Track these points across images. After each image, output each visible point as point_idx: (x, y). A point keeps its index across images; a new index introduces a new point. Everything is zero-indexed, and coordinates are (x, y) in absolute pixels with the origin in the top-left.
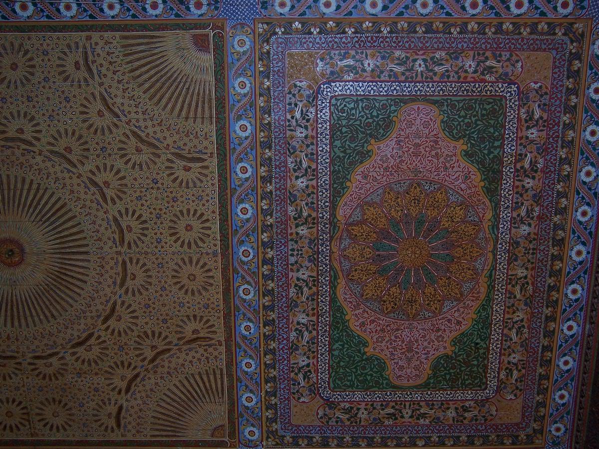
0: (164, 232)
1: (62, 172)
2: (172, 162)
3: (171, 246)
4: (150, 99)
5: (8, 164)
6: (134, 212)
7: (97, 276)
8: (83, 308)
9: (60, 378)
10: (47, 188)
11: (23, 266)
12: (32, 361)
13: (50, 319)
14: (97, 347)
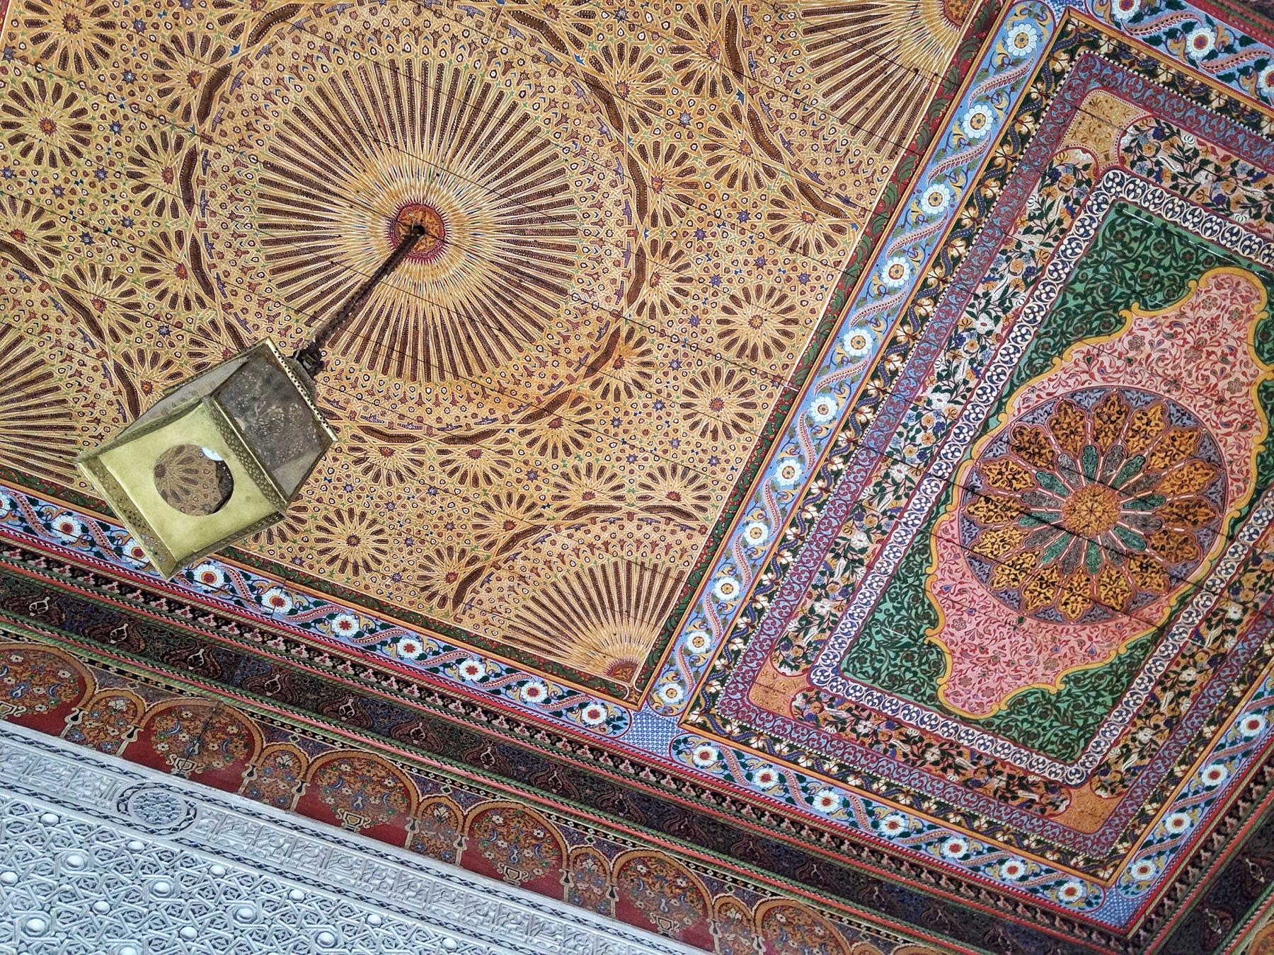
0: (101, 140)
1: (257, 327)
2: (44, 259)
3: (95, 106)
4: (50, 375)
6: (146, 203)
8: (325, 61)
10: (298, 311)
11: (407, 197)
13: (402, 68)
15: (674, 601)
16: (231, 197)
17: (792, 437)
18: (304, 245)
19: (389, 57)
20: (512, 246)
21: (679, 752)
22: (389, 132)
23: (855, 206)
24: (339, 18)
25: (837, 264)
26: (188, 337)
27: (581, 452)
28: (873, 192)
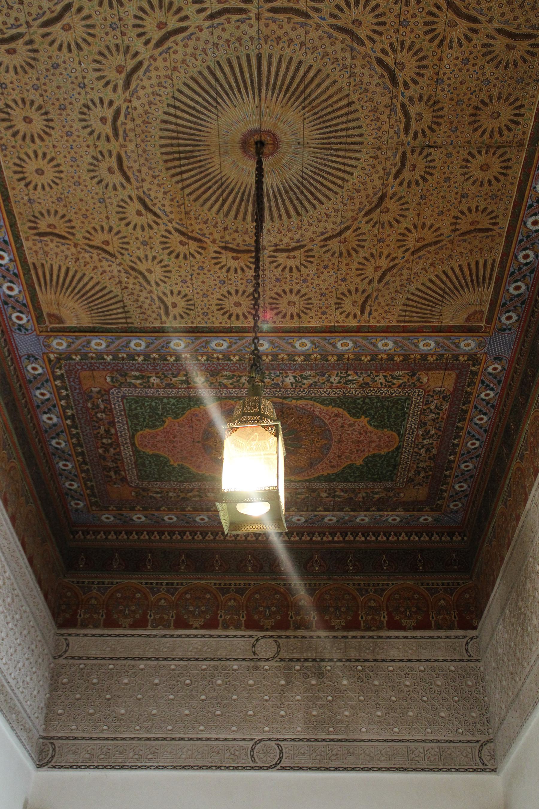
1: (150, 78)
5: (146, 136)
7: (292, 47)
8: (338, 68)
9: (440, 105)
10: (174, 98)
11: (278, 133)
12: (411, 135)
13: (353, 108)
14: (399, 55)
15: (114, 326)
16: (228, 41)
17: (239, 339)
18: (219, 88)
19: (355, 100)
20: (276, 190)
21: (28, 359)
22: (312, 112)
23: (369, 317)
24: (366, 68)
25: (338, 322)
26: (119, 41)
27: (173, 260)
28: (378, 321)
